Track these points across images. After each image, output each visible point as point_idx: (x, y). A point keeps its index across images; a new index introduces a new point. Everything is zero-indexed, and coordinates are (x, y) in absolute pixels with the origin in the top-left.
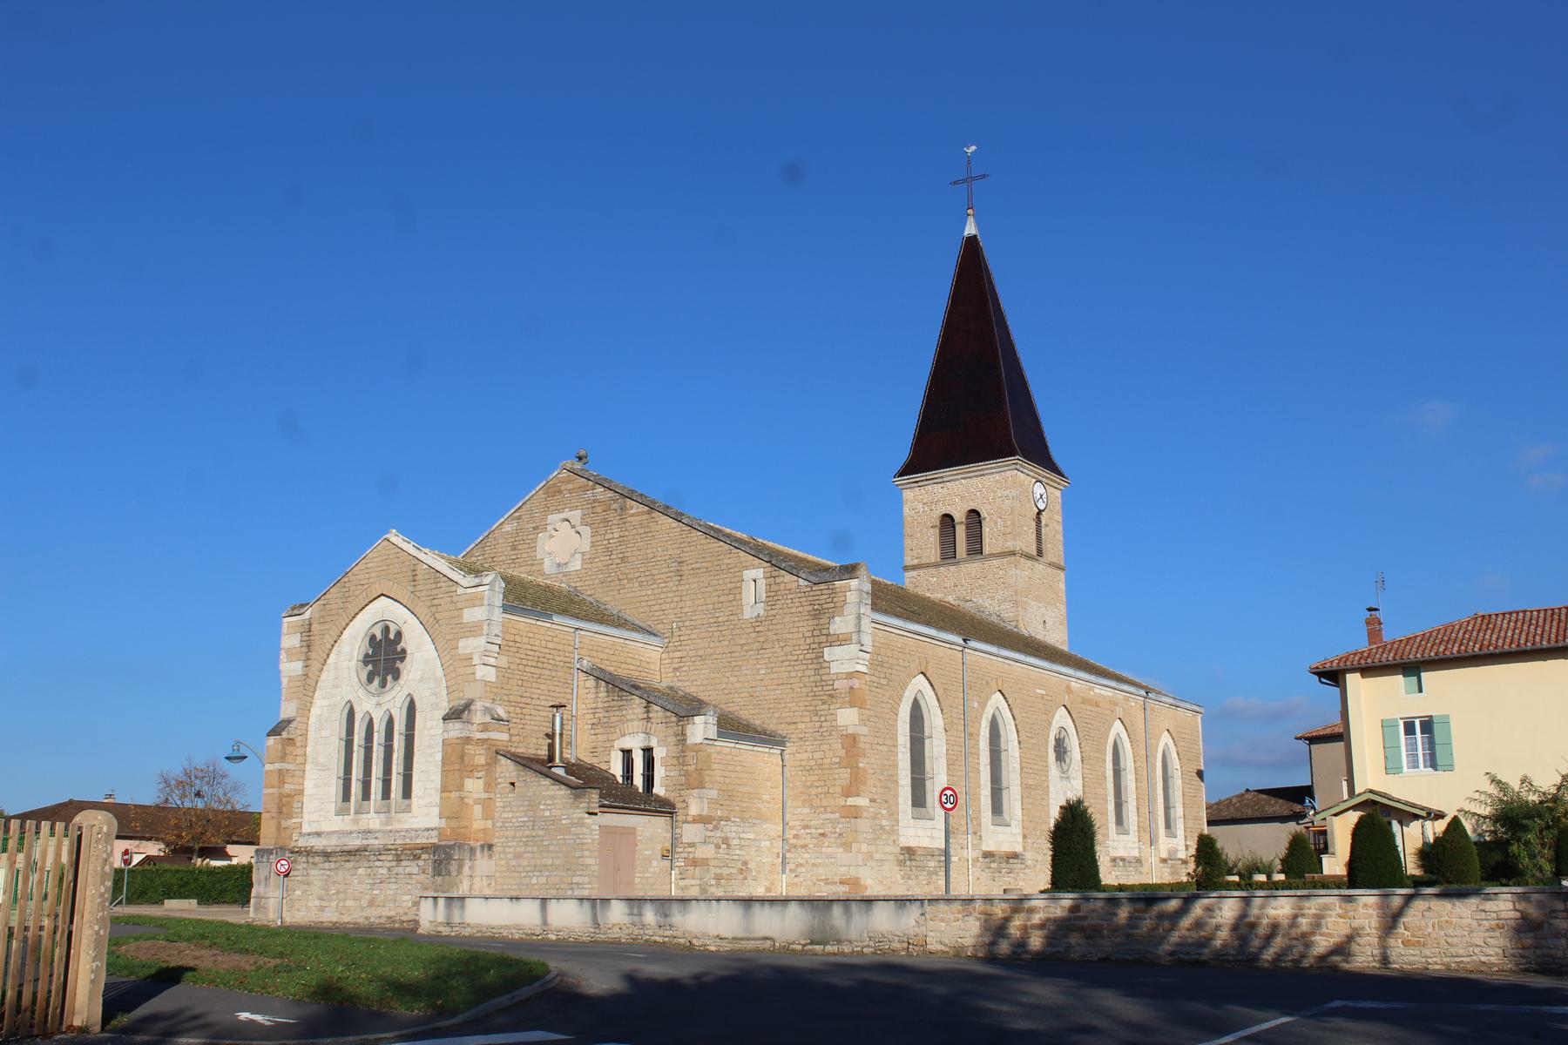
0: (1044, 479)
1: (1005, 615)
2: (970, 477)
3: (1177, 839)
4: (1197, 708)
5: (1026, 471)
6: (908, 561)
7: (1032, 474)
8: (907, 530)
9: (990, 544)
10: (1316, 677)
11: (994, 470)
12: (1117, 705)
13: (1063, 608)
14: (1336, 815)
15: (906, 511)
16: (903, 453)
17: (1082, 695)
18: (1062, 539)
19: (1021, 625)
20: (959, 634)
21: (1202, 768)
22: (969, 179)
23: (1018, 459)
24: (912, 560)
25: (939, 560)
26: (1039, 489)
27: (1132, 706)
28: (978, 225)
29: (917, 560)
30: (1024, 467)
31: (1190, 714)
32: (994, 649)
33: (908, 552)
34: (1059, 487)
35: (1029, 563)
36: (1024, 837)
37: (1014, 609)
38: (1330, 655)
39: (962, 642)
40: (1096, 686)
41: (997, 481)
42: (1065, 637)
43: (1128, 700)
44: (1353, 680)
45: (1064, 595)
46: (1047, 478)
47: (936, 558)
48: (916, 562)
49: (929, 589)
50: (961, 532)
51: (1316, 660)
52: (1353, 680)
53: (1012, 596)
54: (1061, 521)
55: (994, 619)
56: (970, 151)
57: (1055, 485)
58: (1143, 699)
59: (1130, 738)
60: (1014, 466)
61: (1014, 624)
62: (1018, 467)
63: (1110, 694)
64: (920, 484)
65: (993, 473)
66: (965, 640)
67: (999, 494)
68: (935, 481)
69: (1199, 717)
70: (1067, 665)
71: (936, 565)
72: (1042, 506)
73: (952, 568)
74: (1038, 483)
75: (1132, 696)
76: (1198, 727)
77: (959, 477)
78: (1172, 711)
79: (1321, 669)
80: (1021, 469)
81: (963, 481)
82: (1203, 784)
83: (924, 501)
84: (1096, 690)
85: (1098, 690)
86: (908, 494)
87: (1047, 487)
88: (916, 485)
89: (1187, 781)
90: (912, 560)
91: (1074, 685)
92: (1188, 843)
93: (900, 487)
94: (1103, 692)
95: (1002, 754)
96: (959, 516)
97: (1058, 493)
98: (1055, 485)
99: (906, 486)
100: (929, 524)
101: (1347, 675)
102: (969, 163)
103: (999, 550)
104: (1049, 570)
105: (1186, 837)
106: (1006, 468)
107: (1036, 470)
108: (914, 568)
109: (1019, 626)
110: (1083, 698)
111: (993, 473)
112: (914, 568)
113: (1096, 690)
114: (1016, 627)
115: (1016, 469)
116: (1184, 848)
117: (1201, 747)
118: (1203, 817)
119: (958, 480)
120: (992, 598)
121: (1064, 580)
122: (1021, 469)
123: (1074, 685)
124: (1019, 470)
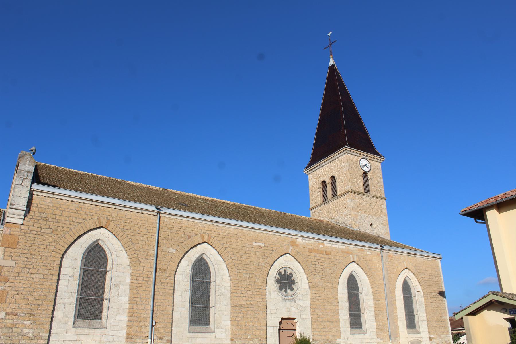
0: (367, 157)
1: (347, 222)
2: (330, 162)
3: (367, 336)
5: (352, 153)
6: (312, 205)
7: (358, 155)
8: (311, 192)
10: (473, 220)
11: (338, 156)
12: (352, 254)
13: (386, 218)
14: (474, 313)
15: (310, 184)
16: (308, 158)
17: (308, 247)
18: (383, 185)
19: (354, 226)
20: (152, 204)
21: (444, 290)
22: (330, 44)
24: (313, 205)
26: (364, 162)
27: (367, 255)
28: (335, 60)
30: (351, 151)
31: (430, 259)
32: (295, 232)
33: (311, 202)
34: (378, 161)
35: (359, 196)
36: (232, 340)
38: (476, 204)
39: (380, 247)
40: (325, 242)
41: (340, 161)
42: (388, 231)
43: (364, 251)
44: (492, 215)
45: (386, 211)
46: (369, 156)
47: (321, 201)
48: (314, 205)
49: (319, 217)
50: (329, 188)
51: (465, 209)
52: (492, 215)
56: (330, 34)
57: (376, 160)
58: (379, 250)
59: (366, 274)
60: (345, 152)
61: (350, 226)
63: (344, 247)
64: (313, 170)
66: (382, 246)
67: (341, 166)
68: (318, 167)
69: (439, 261)
70: (364, 241)
71: (321, 205)
72: (367, 170)
73: (327, 205)
74: (364, 159)
75: (366, 248)
77: (326, 163)
78: (411, 257)
79: (468, 211)
80: (350, 152)
81: (328, 164)
82: (445, 299)
84: (326, 245)
85: (328, 245)
86: (310, 176)
87: (371, 162)
88: (312, 171)
89: (429, 298)
90: (313, 205)
91: (299, 241)
92: (432, 336)
93: (307, 174)
94: (334, 246)
95: (211, 284)
96: (328, 180)
97: (379, 164)
98: (376, 160)
99: (309, 173)
100: (318, 187)
101: (487, 212)
102: (330, 39)
104: (374, 199)
105: (429, 332)
106: (342, 153)
107: (359, 152)
108: (314, 208)
109: (353, 226)
112: (314, 208)
113: (326, 245)
114: (352, 227)
115: (347, 153)
116: (428, 339)
117: (442, 278)
118: (445, 320)
119: (326, 164)
122: (350, 152)
123: (299, 241)
124: (348, 153)
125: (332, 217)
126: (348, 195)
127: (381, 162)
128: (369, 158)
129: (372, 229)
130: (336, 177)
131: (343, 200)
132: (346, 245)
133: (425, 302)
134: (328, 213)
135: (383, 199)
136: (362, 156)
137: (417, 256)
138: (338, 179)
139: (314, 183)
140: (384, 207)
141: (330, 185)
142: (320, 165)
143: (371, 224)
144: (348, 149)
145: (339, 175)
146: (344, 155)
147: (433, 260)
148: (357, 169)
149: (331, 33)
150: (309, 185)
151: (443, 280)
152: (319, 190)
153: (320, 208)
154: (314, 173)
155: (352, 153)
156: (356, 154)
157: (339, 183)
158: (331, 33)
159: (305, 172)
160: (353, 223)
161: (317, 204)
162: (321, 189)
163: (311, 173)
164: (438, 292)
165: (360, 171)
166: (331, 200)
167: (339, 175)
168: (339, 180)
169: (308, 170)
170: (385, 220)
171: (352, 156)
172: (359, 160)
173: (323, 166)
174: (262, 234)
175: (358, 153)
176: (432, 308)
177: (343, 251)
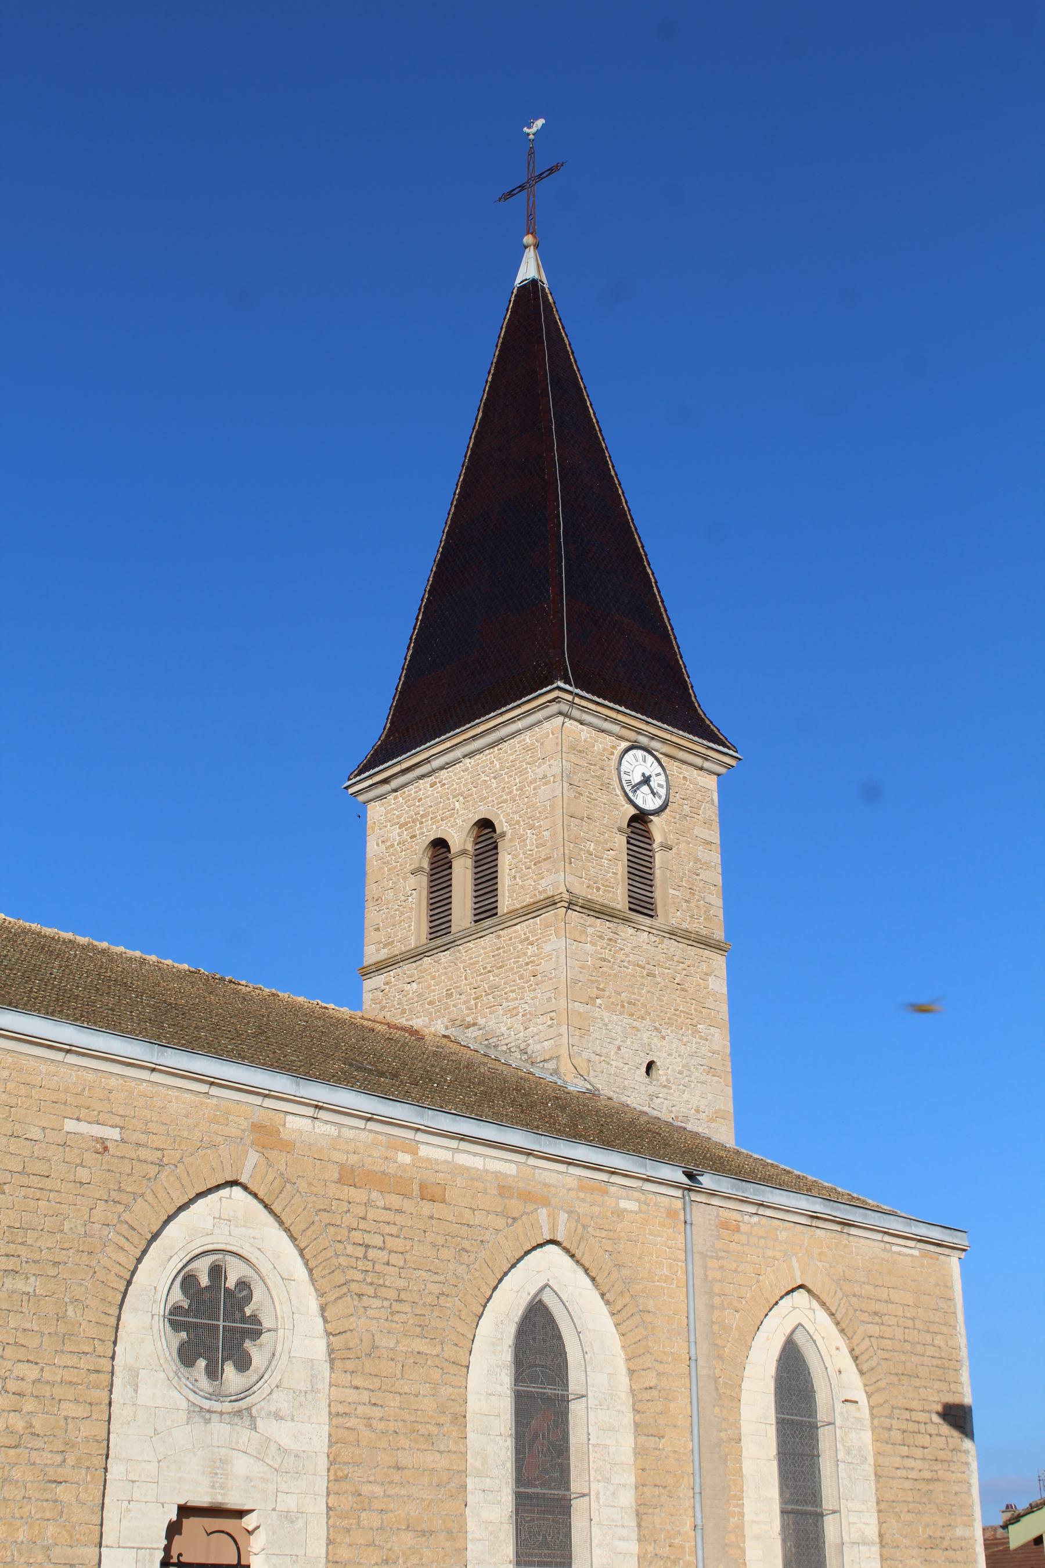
0: (655, 744)
1: (534, 1047)
2: (480, 751)
4: (936, 1234)
5: (586, 717)
6: (372, 954)
7: (616, 729)
8: (372, 889)
9: (511, 891)
11: (519, 725)
12: (546, 1202)
13: (720, 1040)
15: (373, 847)
17: (339, 1157)
18: (719, 879)
19: (566, 1068)
21: (968, 1400)
23: (559, 688)
24: (378, 950)
25: (424, 941)
26: (637, 765)
27: (620, 1213)
28: (546, 261)
29: (386, 951)
30: (583, 709)
31: (914, 1250)
32: (280, 1083)
33: (370, 935)
34: (707, 765)
35: (600, 925)
37: (552, 1033)
39: (685, 1180)
40: (420, 1137)
41: (527, 749)
43: (606, 1192)
45: (724, 1007)
46: (664, 741)
48: (384, 954)
49: (404, 1012)
50: (463, 873)
53: (549, 1000)
54: (716, 839)
55: (515, 1060)
56: (534, 130)
58: (678, 1193)
59: (607, 1303)
60: (554, 708)
61: (551, 1065)
62: (565, 708)
63: (511, 1169)
64: (394, 784)
65: (519, 732)
66: (690, 1176)
69: (954, 1262)
70: (607, 1143)
71: (416, 955)
72: (647, 801)
73: (445, 957)
74: (640, 753)
75: (615, 1179)
76: (949, 1287)
77: (458, 753)
78: (824, 1236)
80: (576, 713)
81: (467, 761)
82: (968, 1444)
83: (402, 820)
84: (424, 1151)
85: (433, 1151)
86: (376, 812)
87: (672, 766)
88: (386, 788)
89: (896, 1436)
90: (378, 950)
93: (362, 798)
96: (459, 839)
97: (711, 783)
98: (699, 761)
100: (409, 868)
102: (531, 154)
103: (528, 900)
104: (672, 946)
106: (540, 715)
107: (620, 717)
108: (381, 967)
109: (562, 1070)
110: (342, 1166)
111: (519, 732)
112: (381, 967)
113: (424, 1151)
114: (556, 1072)
115: (560, 713)
117: (963, 1341)
120: (512, 1012)
121: (724, 973)
124: (566, 715)
125: (469, 1019)
126: (549, 916)
127: (722, 770)
128: (665, 749)
129: (651, 1089)
130: (502, 825)
131: (527, 939)
132: (521, 1158)
133: (878, 1454)
134: (449, 995)
135: (716, 947)
136: (632, 735)
137: (853, 1231)
138: (508, 836)
139: (392, 846)
140: (719, 985)
141: (469, 862)
142: (427, 760)
143: (650, 1066)
144: (570, 697)
145: (516, 817)
146: (546, 725)
147: (925, 1254)
148: (604, 798)
149: (540, 122)
150: (369, 854)
151: (964, 1353)
152: (412, 881)
153: (409, 969)
154: (395, 798)
155: (586, 717)
156: (607, 725)
157: (515, 856)
158: (540, 122)
159: (351, 790)
160: (564, 1052)
161: (398, 948)
162: (424, 880)
163: (381, 797)
164: (940, 1408)
165: (616, 806)
166: (468, 936)
167: (516, 817)
168: (511, 840)
169: (370, 782)
170: (715, 1047)
171: (585, 733)
172: (617, 753)
173: (442, 768)
174: (113, 1082)
175: (615, 721)
176: (908, 1485)
177: (504, 1190)
